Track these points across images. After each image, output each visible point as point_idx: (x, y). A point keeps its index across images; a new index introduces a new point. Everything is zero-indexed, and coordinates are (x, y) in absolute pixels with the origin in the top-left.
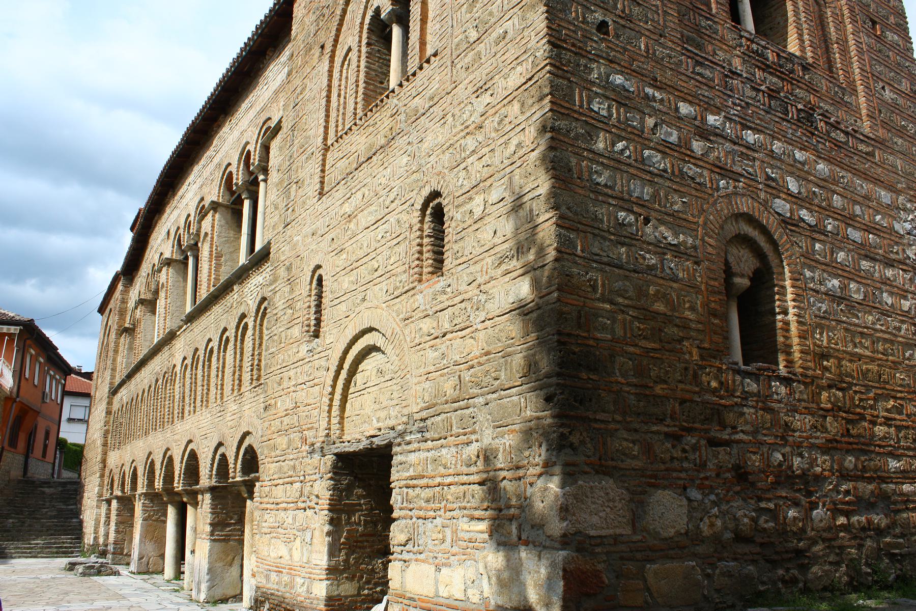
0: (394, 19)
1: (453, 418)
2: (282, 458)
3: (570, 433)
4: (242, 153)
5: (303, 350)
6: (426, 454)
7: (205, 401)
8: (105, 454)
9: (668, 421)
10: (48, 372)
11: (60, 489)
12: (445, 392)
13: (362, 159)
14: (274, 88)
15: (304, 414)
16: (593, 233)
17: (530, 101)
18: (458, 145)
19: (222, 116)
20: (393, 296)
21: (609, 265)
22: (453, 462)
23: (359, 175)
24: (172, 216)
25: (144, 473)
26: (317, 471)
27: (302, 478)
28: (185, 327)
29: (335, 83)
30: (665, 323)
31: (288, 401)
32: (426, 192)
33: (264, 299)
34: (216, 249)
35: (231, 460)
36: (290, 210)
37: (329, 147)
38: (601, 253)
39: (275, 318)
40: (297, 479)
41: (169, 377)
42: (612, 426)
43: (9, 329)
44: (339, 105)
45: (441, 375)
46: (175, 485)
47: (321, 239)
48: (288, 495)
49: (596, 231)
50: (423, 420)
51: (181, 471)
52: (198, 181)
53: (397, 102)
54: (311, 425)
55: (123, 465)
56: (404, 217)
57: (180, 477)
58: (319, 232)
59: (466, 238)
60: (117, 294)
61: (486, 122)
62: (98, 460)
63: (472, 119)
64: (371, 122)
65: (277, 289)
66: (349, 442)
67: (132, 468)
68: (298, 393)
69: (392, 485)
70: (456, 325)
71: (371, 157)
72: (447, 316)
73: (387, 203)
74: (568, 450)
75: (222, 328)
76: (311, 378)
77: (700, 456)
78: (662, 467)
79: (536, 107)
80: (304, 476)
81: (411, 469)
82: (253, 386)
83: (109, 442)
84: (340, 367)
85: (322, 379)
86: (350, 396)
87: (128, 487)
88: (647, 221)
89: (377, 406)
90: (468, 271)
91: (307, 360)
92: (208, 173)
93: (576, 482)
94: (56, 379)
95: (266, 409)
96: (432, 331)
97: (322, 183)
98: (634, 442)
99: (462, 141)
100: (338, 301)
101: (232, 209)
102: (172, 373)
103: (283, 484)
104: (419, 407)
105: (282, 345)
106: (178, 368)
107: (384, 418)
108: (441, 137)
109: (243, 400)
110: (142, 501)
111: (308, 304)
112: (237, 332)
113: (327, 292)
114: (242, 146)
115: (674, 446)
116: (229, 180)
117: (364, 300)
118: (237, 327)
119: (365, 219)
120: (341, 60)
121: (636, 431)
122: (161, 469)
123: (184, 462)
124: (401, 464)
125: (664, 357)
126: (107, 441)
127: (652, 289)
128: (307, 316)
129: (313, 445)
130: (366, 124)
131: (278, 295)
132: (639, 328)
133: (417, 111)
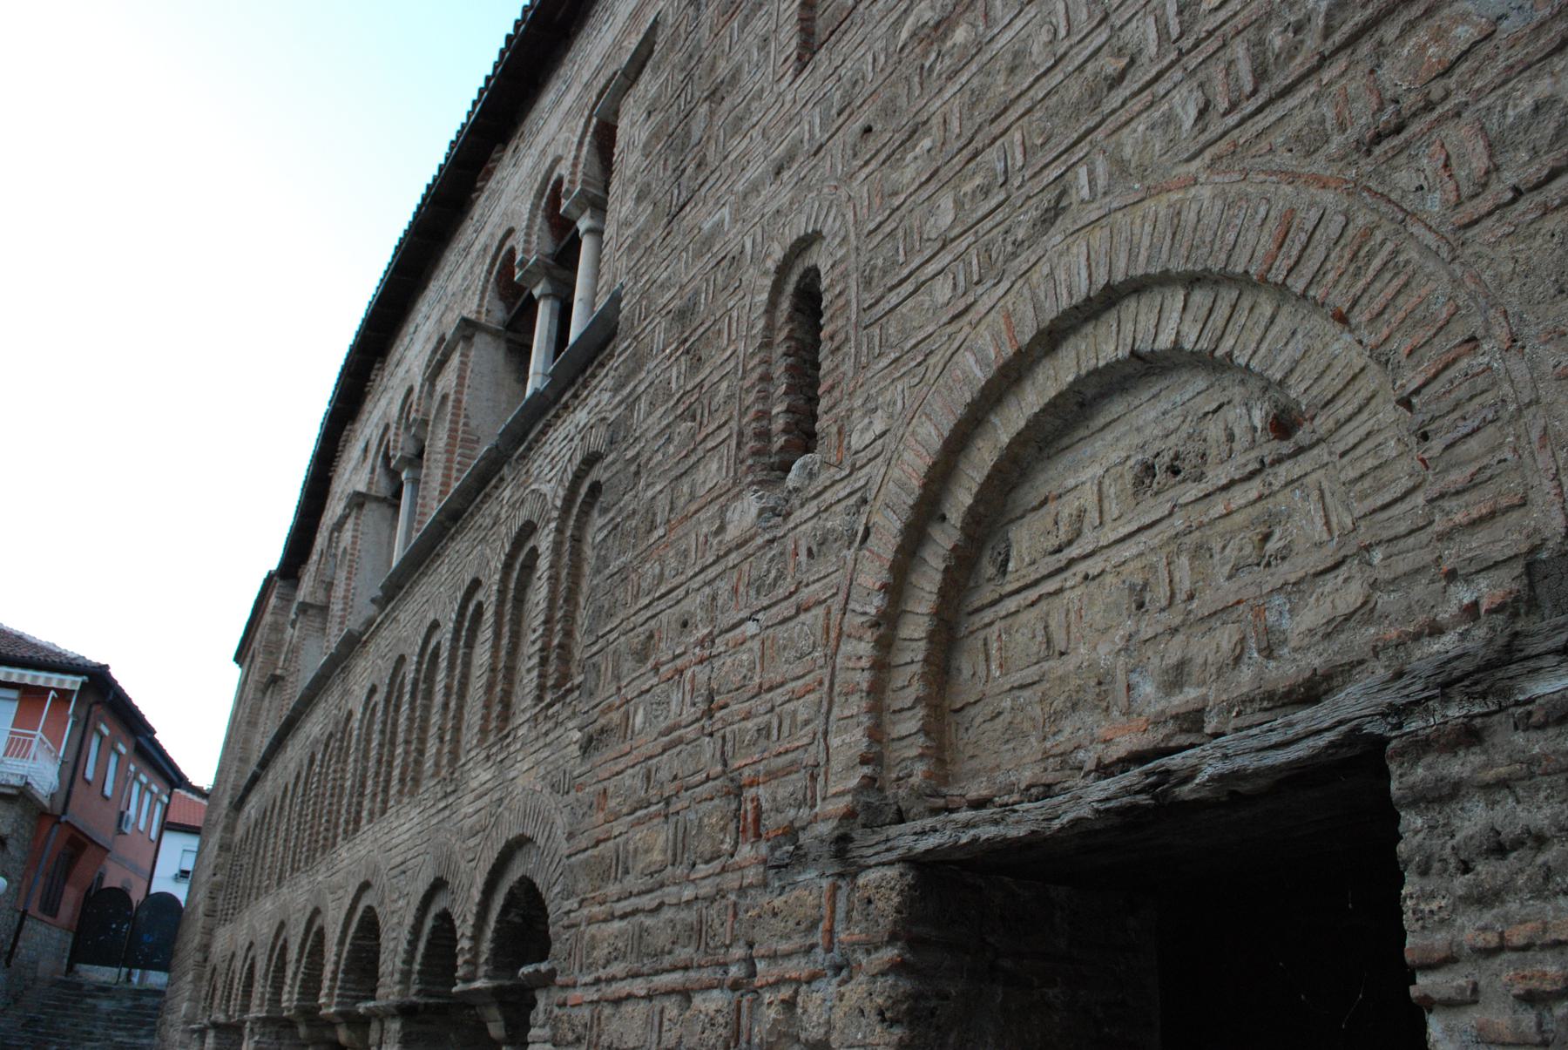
2: (647, 901)
8: (209, 932)
10: (136, 777)
11: (128, 1003)
15: (749, 724)
25: (267, 970)
26: (819, 937)
27: (734, 971)
34: (465, 424)
35: (464, 928)
39: (633, 468)
40: (706, 975)
43: (48, 679)
46: (322, 1000)
51: (337, 963)
57: (334, 979)
60: (268, 618)
67: (249, 961)
68: (717, 663)
69: (1423, 984)
80: (750, 961)
83: (220, 907)
84: (927, 509)
87: (235, 1004)
94: (152, 793)
101: (509, 341)
103: (649, 997)
110: (256, 1038)
112: (504, 581)
118: (508, 567)
122: (299, 961)
123: (348, 940)
126: (215, 905)
129: (791, 832)
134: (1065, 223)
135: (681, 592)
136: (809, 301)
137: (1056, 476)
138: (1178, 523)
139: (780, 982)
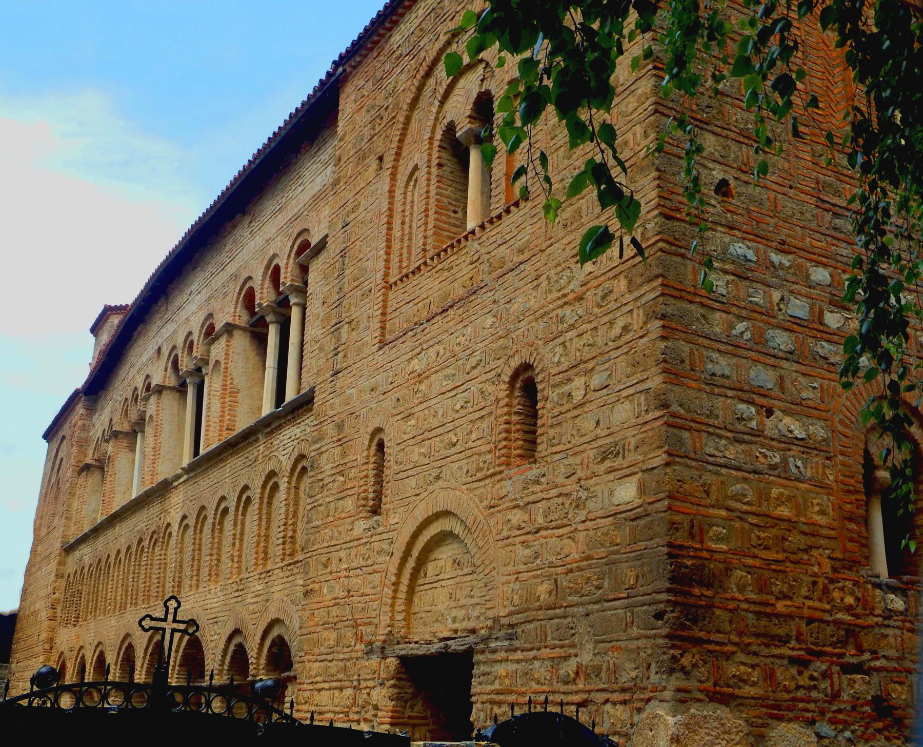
0: (473, 140)
1: (548, 627)
2: (329, 657)
3: (682, 655)
4: (267, 267)
5: (359, 527)
6: (515, 666)
7: (215, 573)
9: (793, 643)
12: (539, 596)
13: (434, 310)
14: (313, 193)
15: (360, 605)
16: (708, 432)
17: (639, 280)
18: (554, 314)
19: (239, 215)
20: (474, 478)
21: (725, 466)
22: (548, 677)
23: (434, 329)
24: (164, 330)
25: (117, 660)
26: (376, 675)
27: (355, 683)
28: (185, 477)
29: (398, 207)
30: (790, 531)
31: (338, 587)
32: (515, 362)
33: (302, 457)
35: (252, 654)
36: (341, 355)
37: (391, 286)
38: (717, 454)
39: (321, 484)
40: (347, 684)
41: (160, 536)
42: (730, 648)
44: (403, 235)
45: (534, 577)
47: (382, 397)
48: (336, 702)
49: (711, 430)
50: (511, 626)
52: (204, 291)
53: (478, 247)
54: (368, 620)
55: (82, 647)
56: (489, 388)
58: (380, 389)
59: (564, 424)
61: (588, 293)
62: (41, 638)
63: (571, 287)
64: (445, 265)
65: (324, 449)
66: (416, 643)
69: (473, 699)
70: (551, 521)
71: (447, 310)
72: (541, 510)
73: (468, 368)
74: (678, 674)
75: (242, 485)
76: (369, 562)
77: (832, 685)
78: (786, 696)
79: (646, 288)
80: (359, 681)
81: (497, 682)
82: (285, 563)
85: (384, 566)
86: (418, 589)
88: (770, 413)
89: (453, 604)
90: (566, 462)
91: (364, 541)
92: (219, 284)
93: (689, 709)
95: (306, 594)
96: (523, 525)
97: (383, 328)
98: (753, 667)
99: (559, 311)
100: (405, 474)
101: (251, 332)
102: (164, 534)
103: (329, 689)
104: (507, 610)
105: (330, 519)
106: (175, 528)
107: (461, 618)
108: (533, 300)
109: (272, 578)
111: (365, 473)
112: (262, 493)
113: (391, 463)
114: (267, 258)
115: (800, 673)
116: (249, 299)
117: (438, 478)
118: (264, 487)
119: (439, 382)
120: (405, 179)
121: (755, 654)
122: (144, 658)
124: (484, 675)
125: (788, 570)
127: (775, 492)
128: (364, 487)
129: (370, 643)
130: (439, 267)
131: (324, 456)
132: (759, 537)
133: (504, 263)
134: (440, 482)
135: (338, 547)
136: (381, 446)
137: (436, 554)
138: (458, 580)
139: (367, 687)
